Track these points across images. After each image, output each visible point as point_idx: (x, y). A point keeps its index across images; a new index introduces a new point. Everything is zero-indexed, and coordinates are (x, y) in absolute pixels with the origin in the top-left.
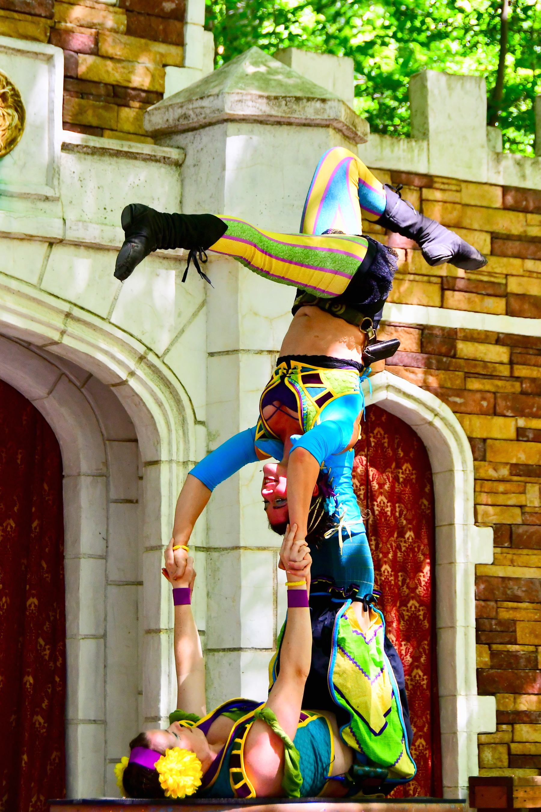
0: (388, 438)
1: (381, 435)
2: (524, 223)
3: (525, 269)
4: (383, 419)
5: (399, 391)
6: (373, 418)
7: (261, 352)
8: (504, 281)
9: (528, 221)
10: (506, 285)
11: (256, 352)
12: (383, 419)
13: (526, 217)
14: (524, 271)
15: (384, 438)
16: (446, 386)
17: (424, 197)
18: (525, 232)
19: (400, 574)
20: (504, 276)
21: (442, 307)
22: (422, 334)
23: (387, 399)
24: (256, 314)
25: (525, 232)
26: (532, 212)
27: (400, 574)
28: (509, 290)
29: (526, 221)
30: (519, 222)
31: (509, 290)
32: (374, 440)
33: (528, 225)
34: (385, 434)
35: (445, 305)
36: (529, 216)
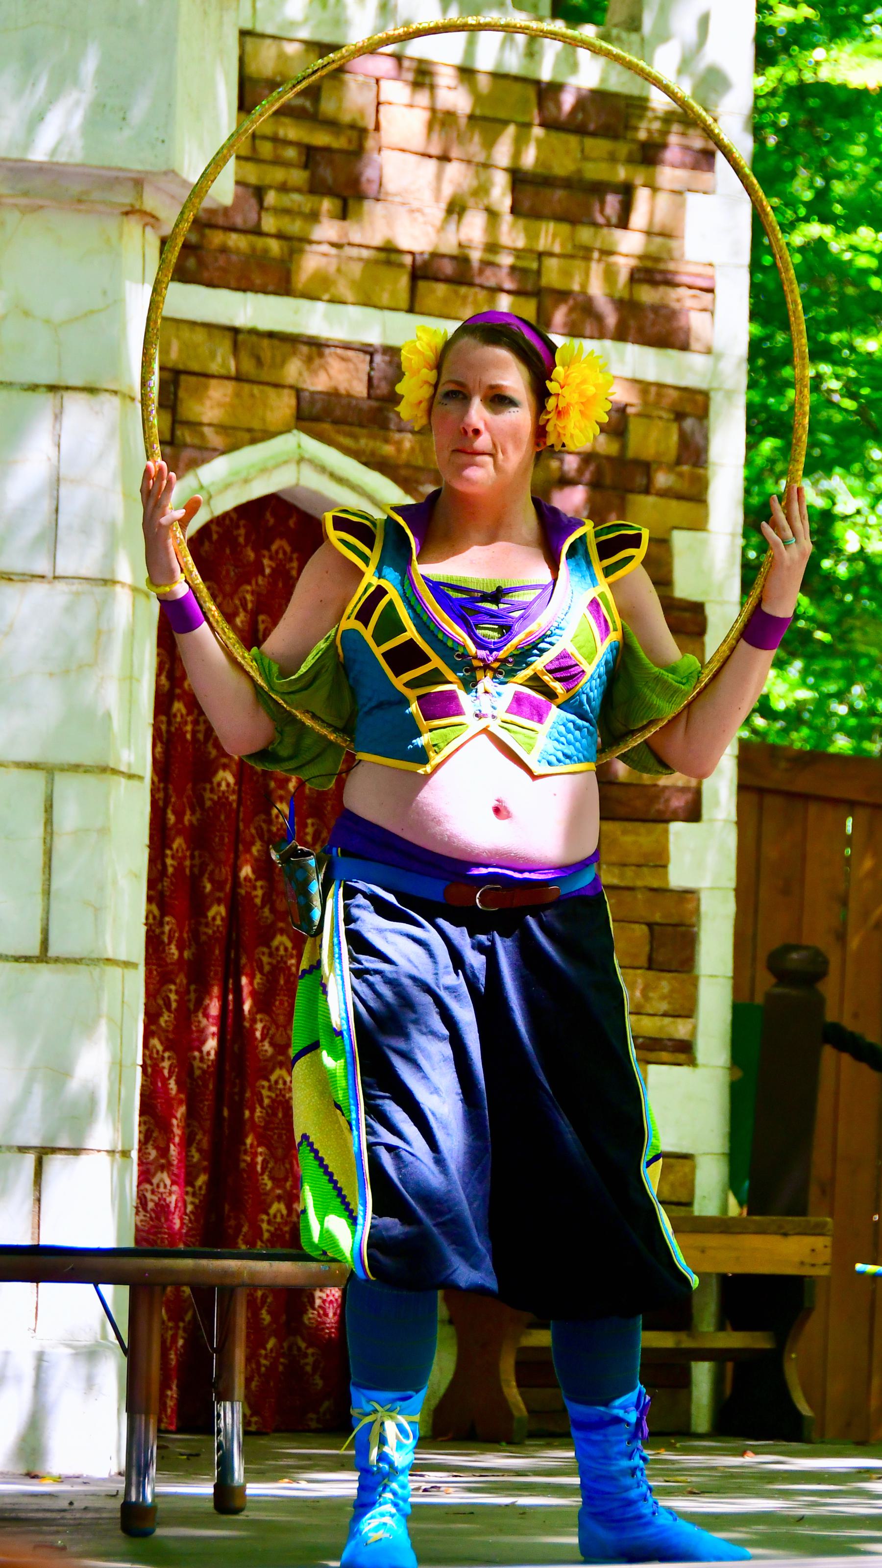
0: (298, 559)
1: (285, 553)
2: (579, 155)
3: (577, 243)
4: (292, 523)
5: (322, 469)
6: (272, 521)
7: (34, 388)
8: (534, 265)
9: (587, 150)
10: (539, 272)
11: (26, 387)
12: (292, 523)
13: (582, 143)
14: (574, 246)
15: (291, 560)
16: (414, 463)
17: (383, 98)
18: (579, 171)
19: (309, 821)
20: (535, 256)
21: (411, 310)
22: (371, 361)
23: (297, 485)
24: (27, 314)
25: (579, 171)
26: (594, 134)
27: (309, 821)
28: (544, 281)
29: (582, 151)
30: (567, 152)
31: (544, 281)
32: (271, 563)
33: (585, 158)
34: (292, 552)
35: (417, 308)
36: (589, 142)
